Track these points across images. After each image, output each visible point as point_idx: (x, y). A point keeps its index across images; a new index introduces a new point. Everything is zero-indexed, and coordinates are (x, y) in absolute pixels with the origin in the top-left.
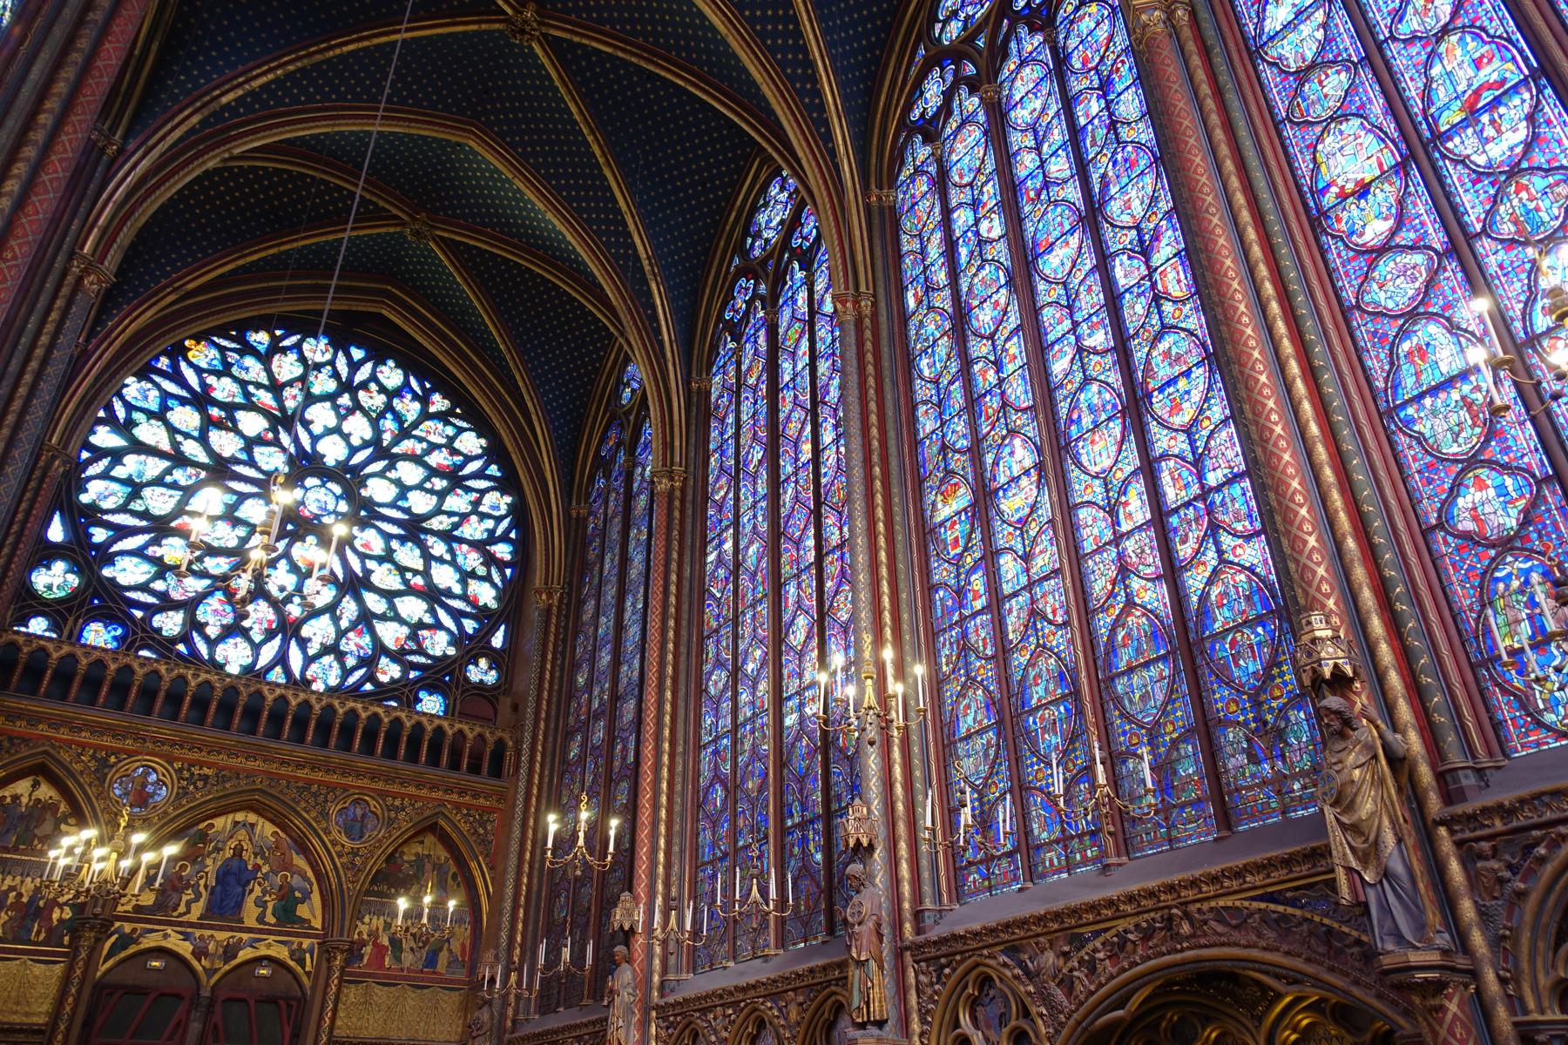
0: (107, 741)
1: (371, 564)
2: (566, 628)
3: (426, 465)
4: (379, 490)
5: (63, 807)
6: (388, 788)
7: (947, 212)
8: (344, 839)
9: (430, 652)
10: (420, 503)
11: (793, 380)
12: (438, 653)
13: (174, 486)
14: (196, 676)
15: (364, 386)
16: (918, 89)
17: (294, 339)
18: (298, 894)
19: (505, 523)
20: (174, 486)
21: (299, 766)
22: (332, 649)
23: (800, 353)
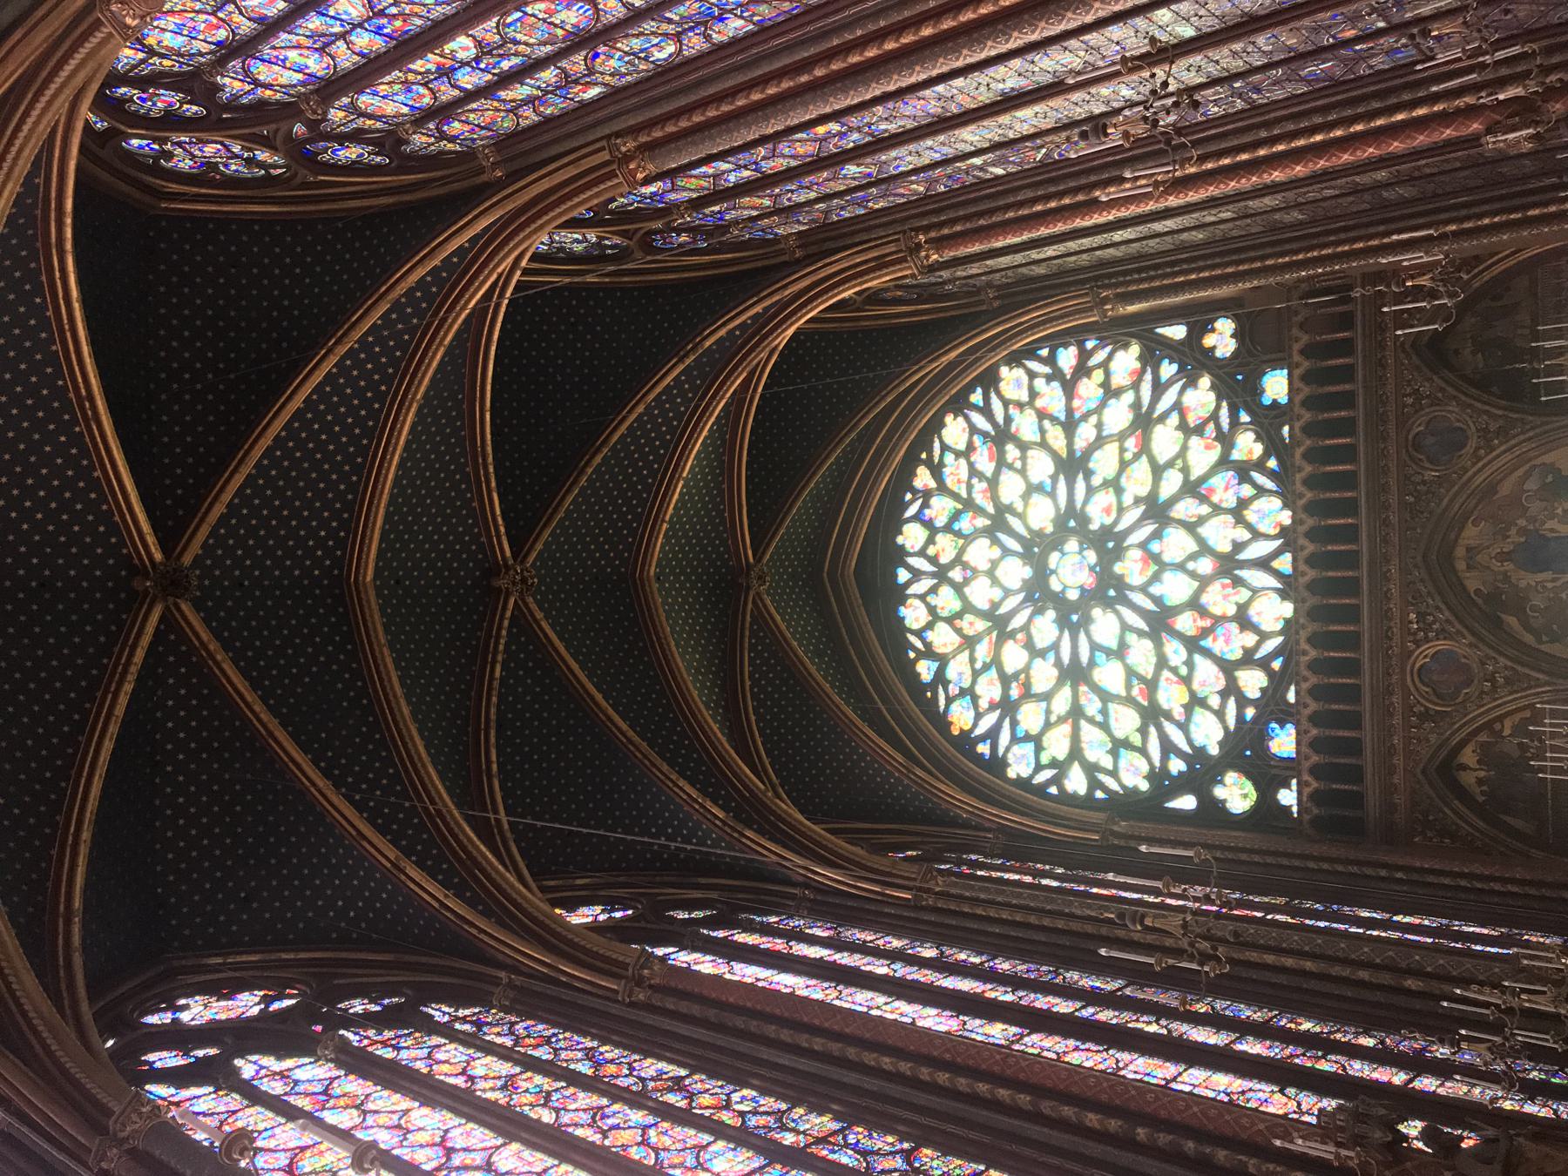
0: (1397, 720)
1: (1128, 499)
2: (1139, 270)
3: (997, 472)
4: (1041, 514)
5: (1483, 737)
7: (471, 95)
8: (1469, 449)
10: (1041, 467)
11: (745, 167)
13: (1104, 712)
14: (1305, 653)
15: (933, 560)
16: (353, 168)
17: (912, 638)
18: (1550, 479)
19: (1033, 365)
20: (1104, 712)
21: (1386, 523)
22: (1238, 512)
23: (711, 171)
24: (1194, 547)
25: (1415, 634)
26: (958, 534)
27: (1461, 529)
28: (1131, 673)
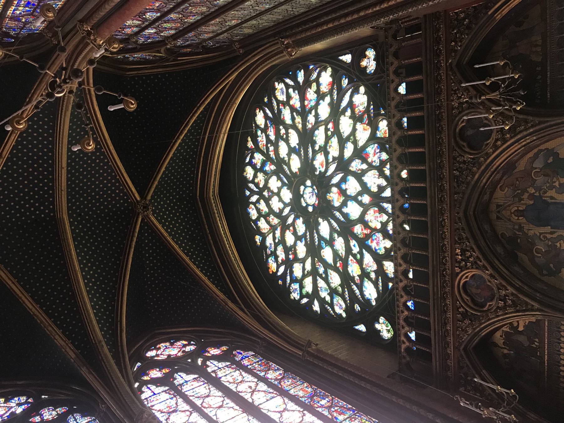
0: (450, 315)
6: (445, 115)
9: (366, 105)
12: (365, 98)
13: (326, 272)
18: (551, 160)
19: (288, 81)
20: (326, 272)
21: (441, 189)
24: (359, 188)
25: (460, 263)
26: (265, 173)
27: (492, 194)
28: (336, 254)
